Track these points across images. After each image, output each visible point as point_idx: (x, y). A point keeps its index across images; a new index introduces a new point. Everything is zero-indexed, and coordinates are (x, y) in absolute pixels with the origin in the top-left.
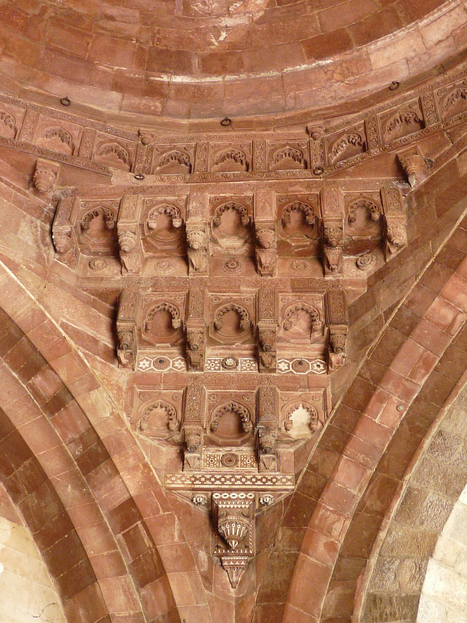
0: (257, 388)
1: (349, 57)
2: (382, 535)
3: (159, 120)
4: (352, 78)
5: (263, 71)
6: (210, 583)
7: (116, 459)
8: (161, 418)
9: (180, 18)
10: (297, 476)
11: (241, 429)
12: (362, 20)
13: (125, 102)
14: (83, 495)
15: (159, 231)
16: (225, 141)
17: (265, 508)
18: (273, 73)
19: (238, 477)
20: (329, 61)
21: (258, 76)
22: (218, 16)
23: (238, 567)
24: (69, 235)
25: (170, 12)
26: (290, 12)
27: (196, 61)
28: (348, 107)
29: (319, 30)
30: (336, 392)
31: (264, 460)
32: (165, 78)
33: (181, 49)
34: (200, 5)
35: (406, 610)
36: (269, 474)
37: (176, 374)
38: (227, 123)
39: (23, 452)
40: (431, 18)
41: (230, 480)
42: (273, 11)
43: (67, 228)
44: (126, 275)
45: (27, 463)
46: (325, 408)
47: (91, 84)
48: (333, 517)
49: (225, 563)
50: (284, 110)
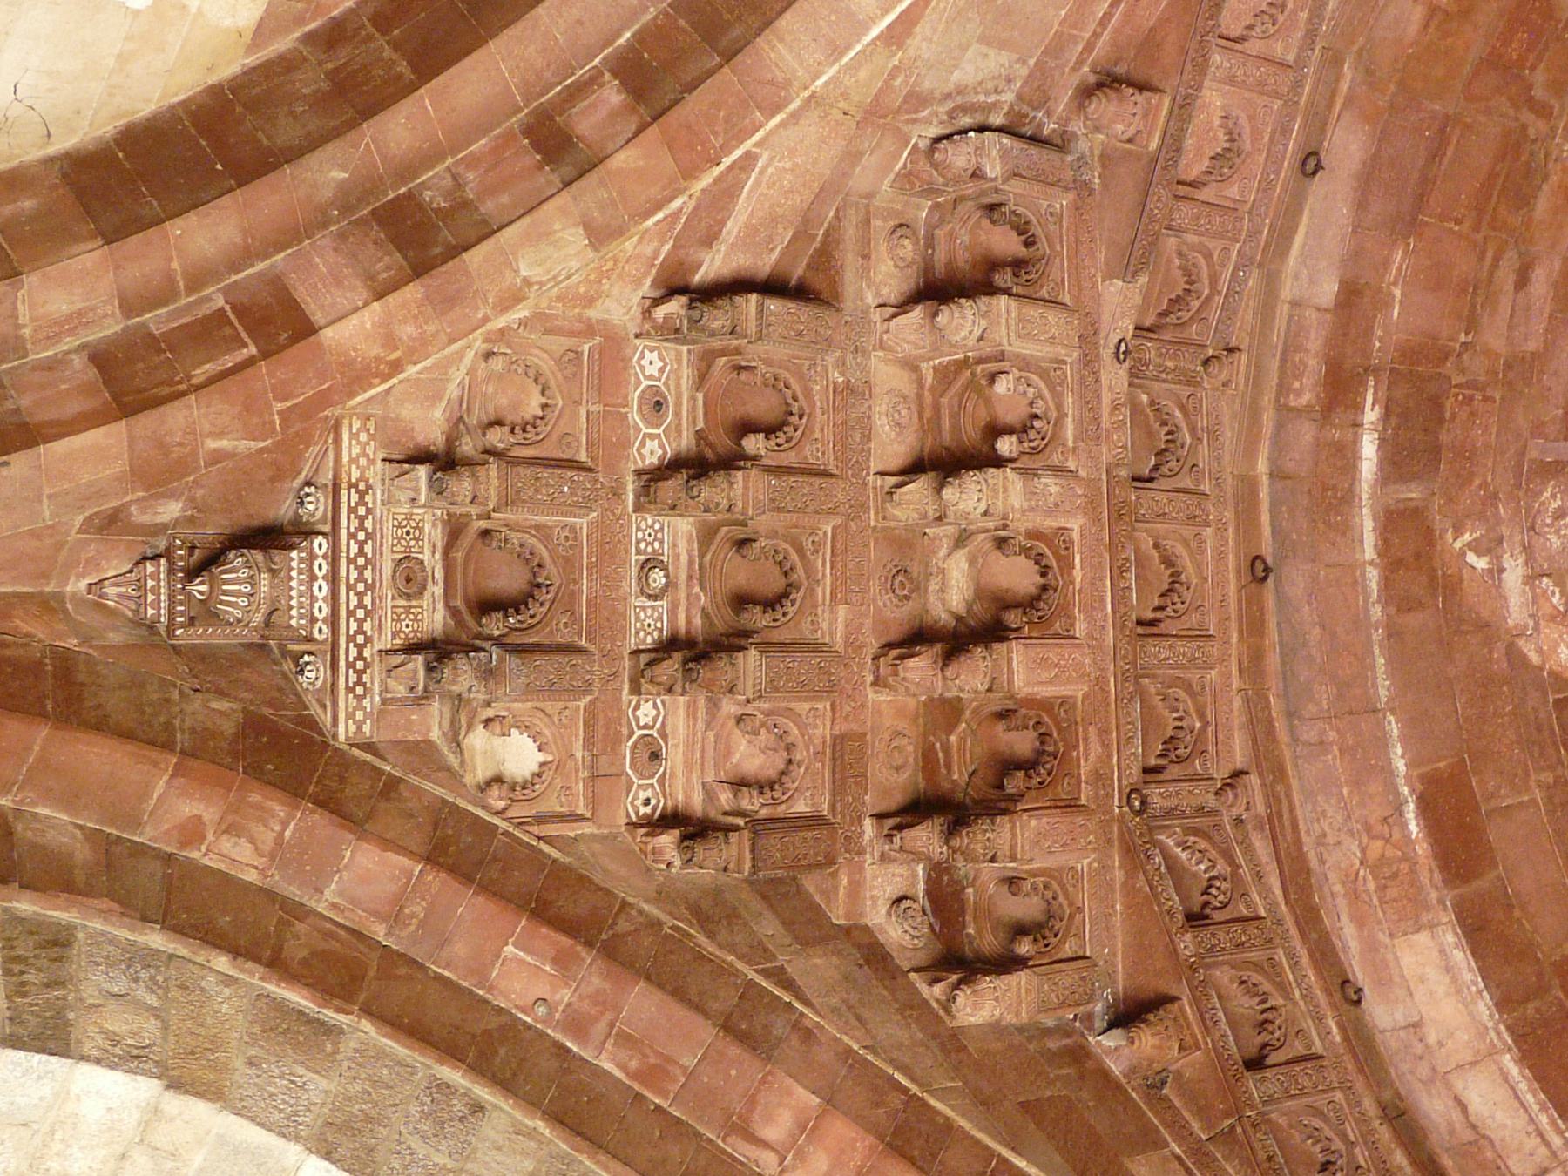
0: (592, 648)
1: (1424, 878)
2: (222, 962)
3: (1267, 400)
4: (1371, 886)
6: (100, 530)
7: (412, 292)
8: (515, 406)
9: (1522, 453)
10: (369, 747)
11: (487, 606)
12: (1517, 913)
13: (1311, 315)
14: (323, 210)
15: (988, 401)
16: (1213, 567)
17: (288, 666)
18: (1383, 689)
19: (367, 600)
20: (1413, 828)
21: (1376, 650)
22: (1527, 549)
23: (141, 600)
24: (977, 175)
25: (1538, 429)
26: (1539, 729)
27: (1413, 493)
28: (1298, 876)
29: (1493, 804)
30: (582, 847)
31: (410, 666)
32: (1371, 415)
33: (1446, 455)
35: (32, 1022)
36: (374, 678)
37: (625, 444)
38: (1258, 571)
39: (432, 58)
40: (1523, 1086)
41: (361, 578)
42: (1541, 688)
43: (993, 169)
44: (876, 316)
45: (403, 67)
46: (541, 820)
48: (267, 838)
49: (150, 568)
50: (1290, 715)
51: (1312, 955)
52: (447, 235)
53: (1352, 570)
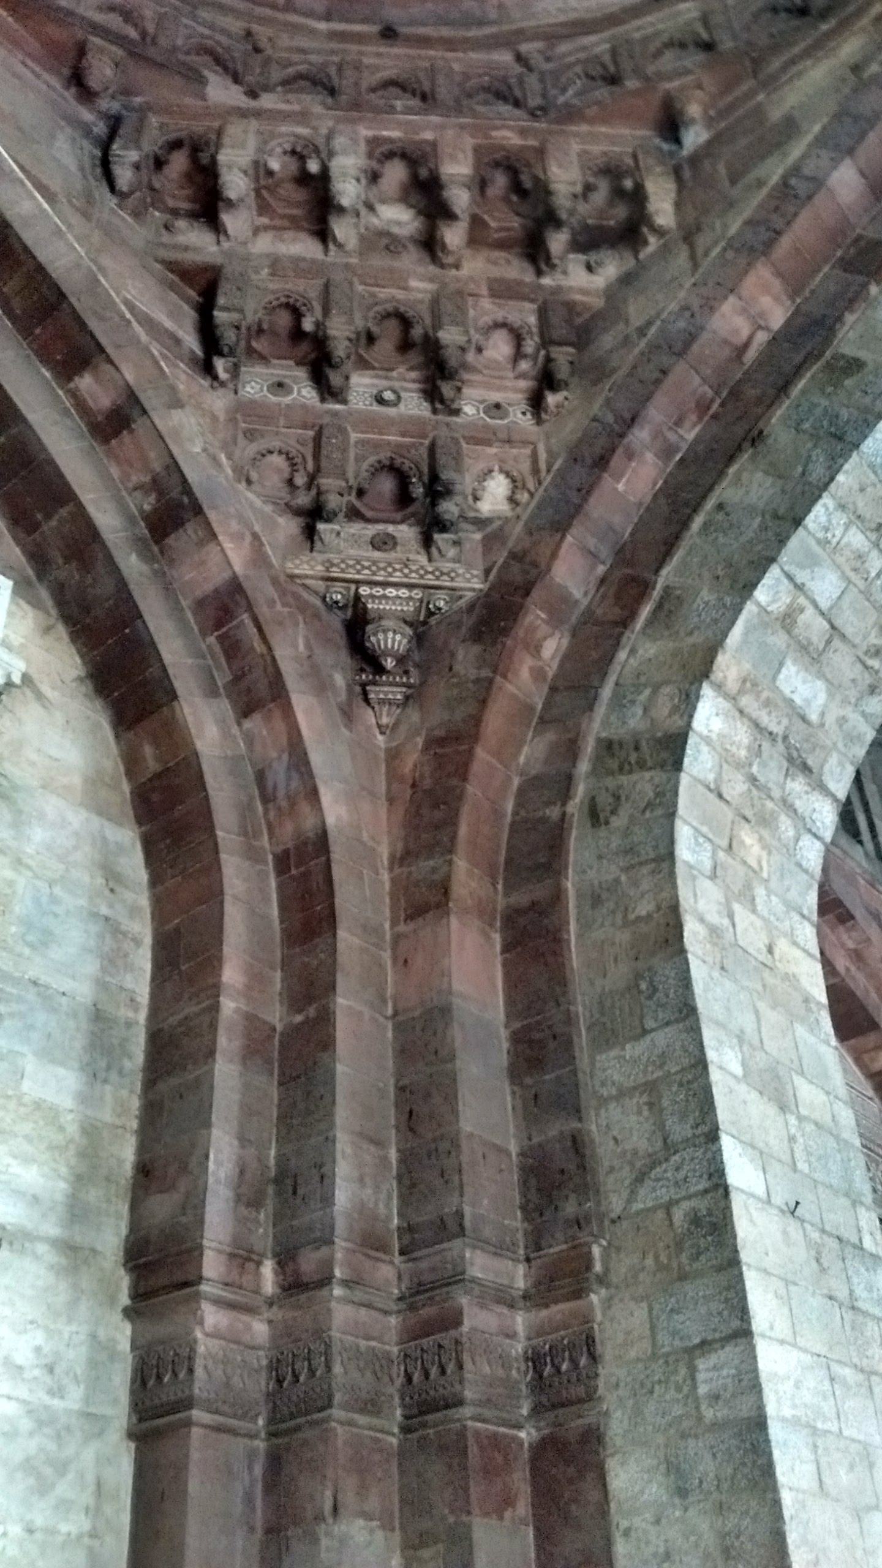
0: (431, 435)
2: (622, 655)
6: (351, 721)
7: (212, 515)
8: (279, 471)
10: (487, 572)
11: (403, 498)
14: (155, 572)
15: (282, 181)
17: (433, 621)
19: (397, 566)
23: (390, 703)
24: (137, 167)
30: (555, 449)
31: (440, 543)
35: (664, 755)
36: (447, 566)
37: (304, 406)
39: (58, 492)
41: (384, 569)
43: (133, 156)
44: (226, 245)
45: (63, 512)
46: (536, 471)
48: (544, 629)
49: (372, 696)
52: (175, 494)
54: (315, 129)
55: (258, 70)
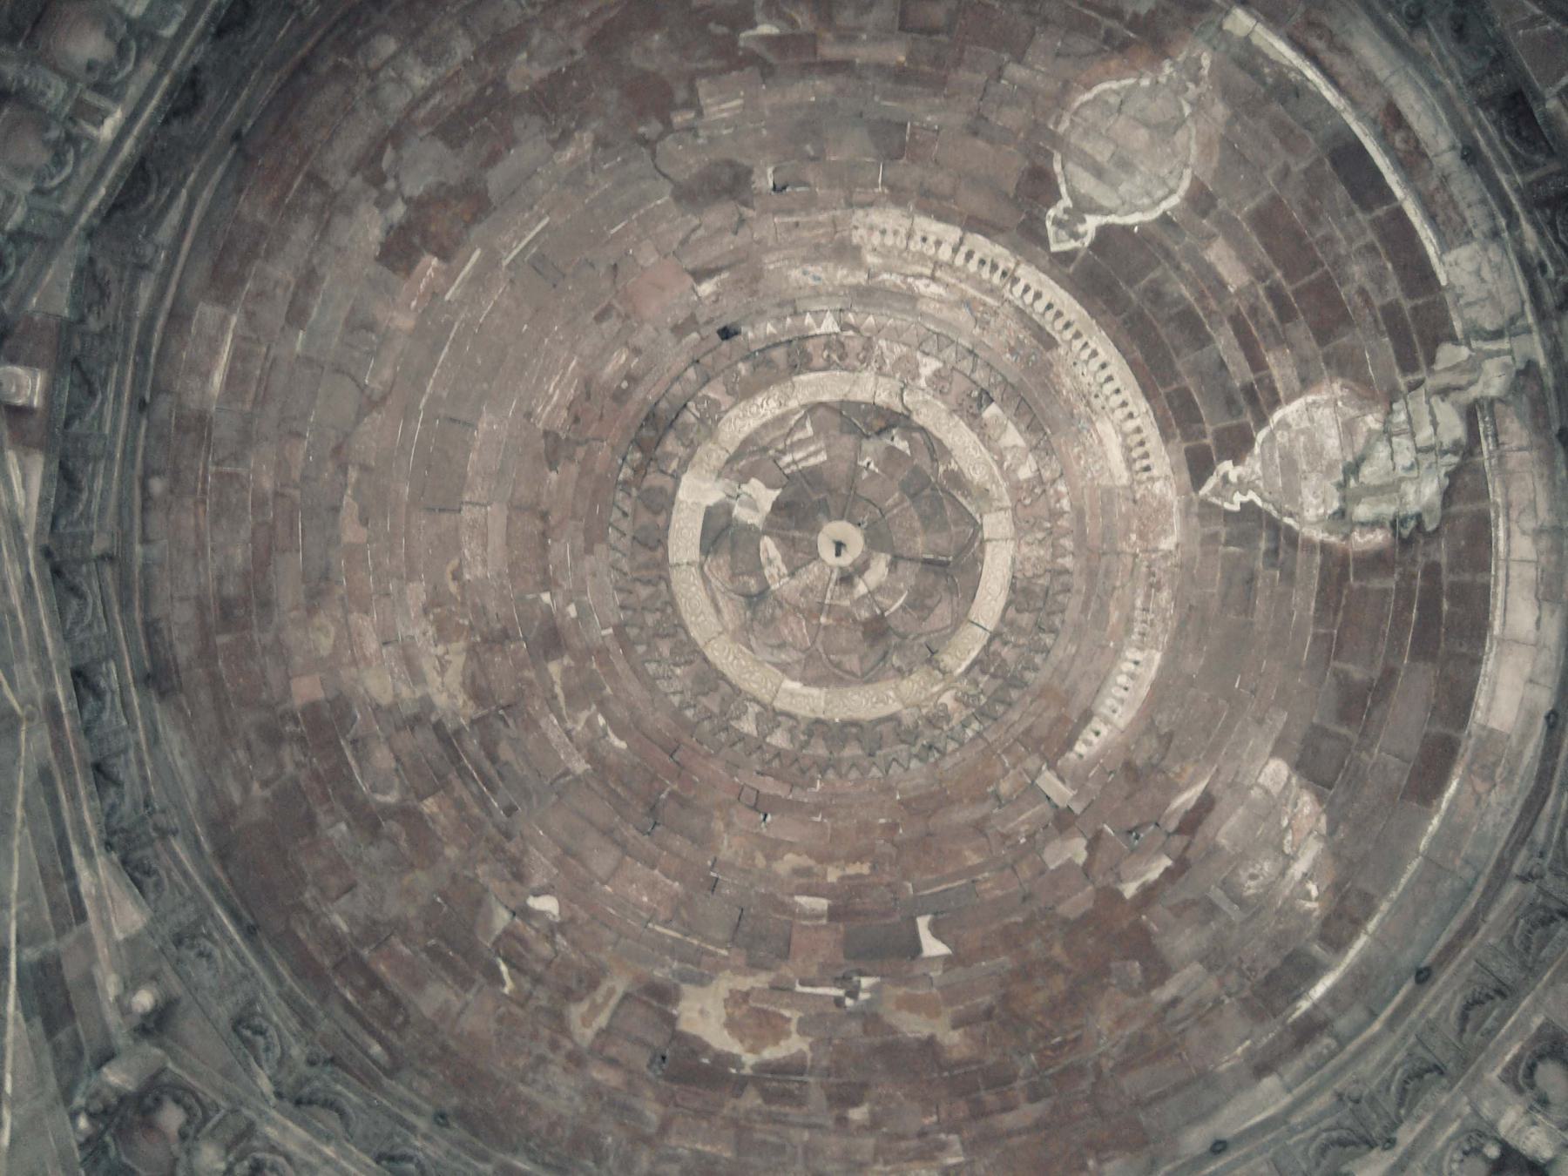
4: (1499, 770)
5: (1401, 876)
9: (1248, 920)
12: (1433, 701)
13: (1287, 1078)
16: (1444, 997)
18: (1413, 866)
21: (1400, 888)
22: (1283, 873)
25: (1230, 925)
27: (1316, 949)
32: (1304, 1005)
34: (1252, 883)
38: (1423, 976)
40: (1498, 613)
42: (1331, 803)
47: (1229, 1098)
50: (1470, 890)
51: (1557, 755)
53: (1377, 939)
54: (1459, 1116)
55: (1374, 1116)
